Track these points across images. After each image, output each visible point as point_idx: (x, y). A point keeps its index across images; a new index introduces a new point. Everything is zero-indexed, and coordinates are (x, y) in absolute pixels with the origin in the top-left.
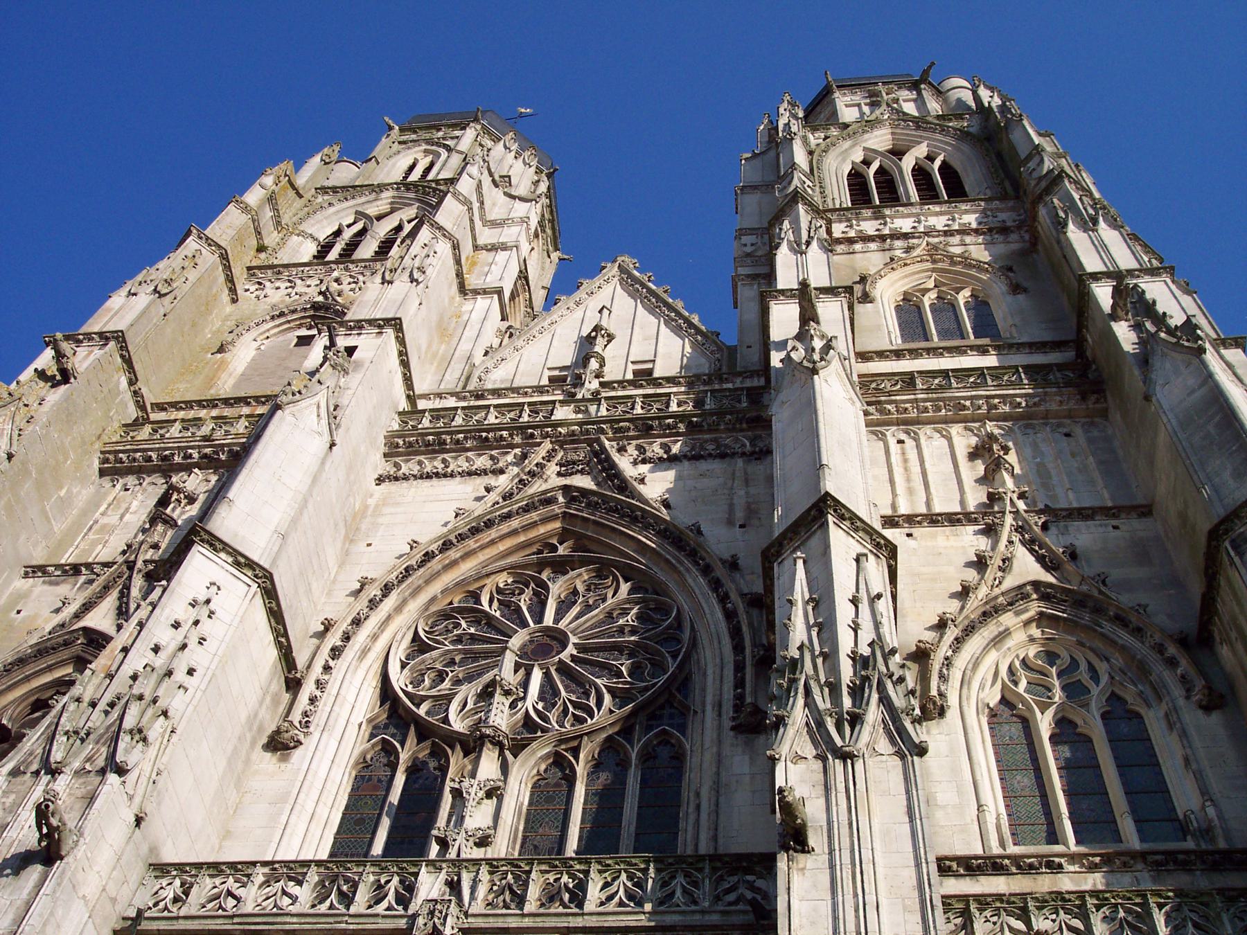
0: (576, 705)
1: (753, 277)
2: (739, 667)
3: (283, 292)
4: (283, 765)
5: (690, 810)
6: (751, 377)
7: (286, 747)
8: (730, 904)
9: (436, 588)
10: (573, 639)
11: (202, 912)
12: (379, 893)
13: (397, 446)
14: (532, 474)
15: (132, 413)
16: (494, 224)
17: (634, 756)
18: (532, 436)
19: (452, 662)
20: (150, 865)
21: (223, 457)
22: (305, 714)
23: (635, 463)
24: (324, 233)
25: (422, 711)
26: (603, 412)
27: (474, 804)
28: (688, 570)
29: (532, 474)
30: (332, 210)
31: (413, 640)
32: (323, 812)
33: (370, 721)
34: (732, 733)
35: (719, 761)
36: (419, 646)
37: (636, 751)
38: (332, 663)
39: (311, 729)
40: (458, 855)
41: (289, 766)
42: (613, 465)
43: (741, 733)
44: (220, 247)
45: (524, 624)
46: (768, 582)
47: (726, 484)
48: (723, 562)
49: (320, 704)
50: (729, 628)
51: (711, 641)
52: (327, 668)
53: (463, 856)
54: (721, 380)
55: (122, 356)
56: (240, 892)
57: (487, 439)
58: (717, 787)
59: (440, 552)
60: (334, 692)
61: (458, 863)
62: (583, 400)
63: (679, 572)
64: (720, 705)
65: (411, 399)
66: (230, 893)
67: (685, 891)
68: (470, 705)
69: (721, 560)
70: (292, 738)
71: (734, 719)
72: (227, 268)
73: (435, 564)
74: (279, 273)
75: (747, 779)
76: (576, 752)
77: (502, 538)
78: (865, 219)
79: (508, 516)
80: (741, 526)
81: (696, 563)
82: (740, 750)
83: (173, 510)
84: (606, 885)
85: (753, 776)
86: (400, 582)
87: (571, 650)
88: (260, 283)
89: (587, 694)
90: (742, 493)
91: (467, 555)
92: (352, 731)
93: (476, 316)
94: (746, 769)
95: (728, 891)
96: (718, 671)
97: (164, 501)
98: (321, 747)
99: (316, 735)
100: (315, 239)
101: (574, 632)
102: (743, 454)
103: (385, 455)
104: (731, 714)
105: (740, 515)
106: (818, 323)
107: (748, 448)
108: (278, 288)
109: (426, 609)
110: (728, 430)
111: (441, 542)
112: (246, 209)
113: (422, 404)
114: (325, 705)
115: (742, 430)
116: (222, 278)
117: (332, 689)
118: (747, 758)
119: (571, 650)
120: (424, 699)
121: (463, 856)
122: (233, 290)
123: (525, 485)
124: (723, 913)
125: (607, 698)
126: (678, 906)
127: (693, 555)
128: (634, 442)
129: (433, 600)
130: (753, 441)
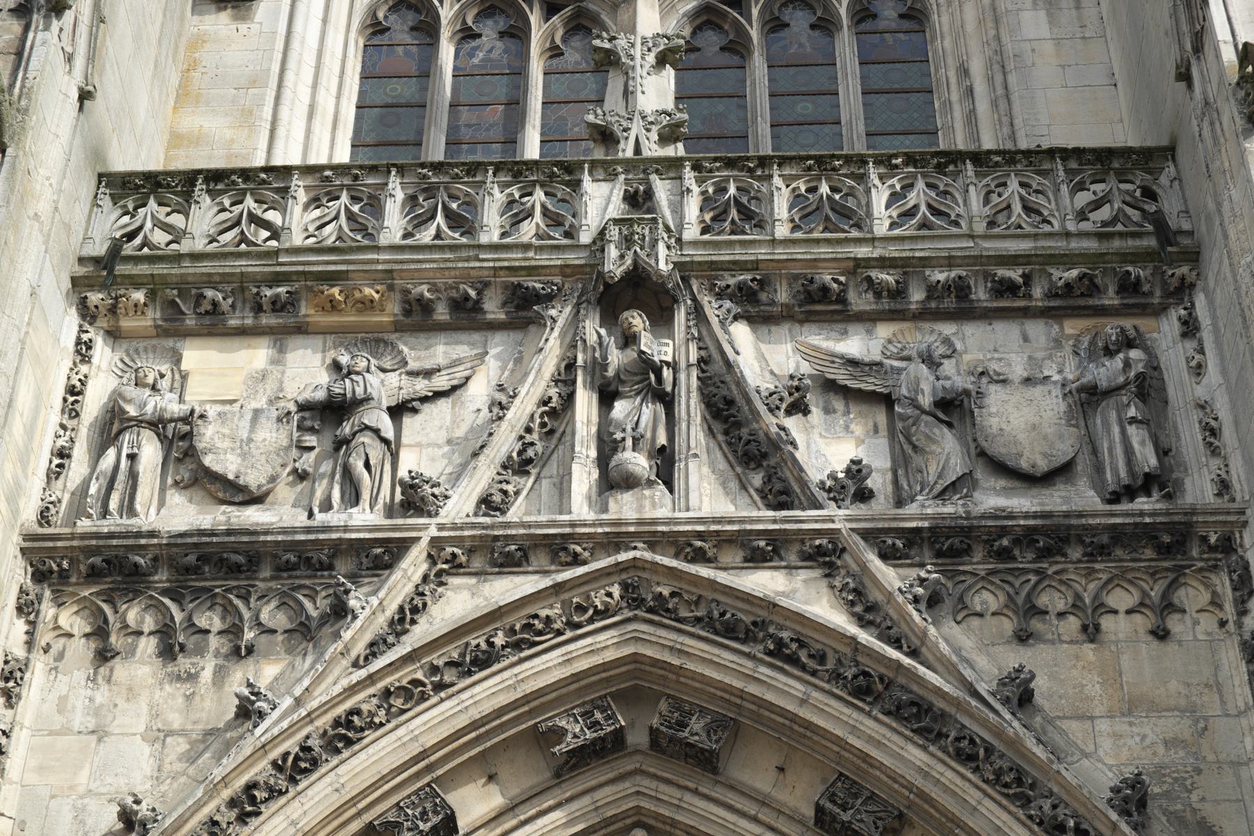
4: (243, 27)
5: (955, 97)
8: (1105, 224)
12: (516, 215)
17: (843, 11)
20: (100, 176)
32: (326, 102)
40: (638, 150)
53: (646, 153)
56: (273, 216)
58: (999, 63)
61: (641, 165)
66: (254, 219)
67: (1028, 209)
75: (1049, 47)
84: (894, 198)
85: (1058, 41)
94: (1044, 31)
95: (1097, 205)
118: (1042, 14)
121: (646, 153)
124: (1101, 236)
126: (1020, 227)
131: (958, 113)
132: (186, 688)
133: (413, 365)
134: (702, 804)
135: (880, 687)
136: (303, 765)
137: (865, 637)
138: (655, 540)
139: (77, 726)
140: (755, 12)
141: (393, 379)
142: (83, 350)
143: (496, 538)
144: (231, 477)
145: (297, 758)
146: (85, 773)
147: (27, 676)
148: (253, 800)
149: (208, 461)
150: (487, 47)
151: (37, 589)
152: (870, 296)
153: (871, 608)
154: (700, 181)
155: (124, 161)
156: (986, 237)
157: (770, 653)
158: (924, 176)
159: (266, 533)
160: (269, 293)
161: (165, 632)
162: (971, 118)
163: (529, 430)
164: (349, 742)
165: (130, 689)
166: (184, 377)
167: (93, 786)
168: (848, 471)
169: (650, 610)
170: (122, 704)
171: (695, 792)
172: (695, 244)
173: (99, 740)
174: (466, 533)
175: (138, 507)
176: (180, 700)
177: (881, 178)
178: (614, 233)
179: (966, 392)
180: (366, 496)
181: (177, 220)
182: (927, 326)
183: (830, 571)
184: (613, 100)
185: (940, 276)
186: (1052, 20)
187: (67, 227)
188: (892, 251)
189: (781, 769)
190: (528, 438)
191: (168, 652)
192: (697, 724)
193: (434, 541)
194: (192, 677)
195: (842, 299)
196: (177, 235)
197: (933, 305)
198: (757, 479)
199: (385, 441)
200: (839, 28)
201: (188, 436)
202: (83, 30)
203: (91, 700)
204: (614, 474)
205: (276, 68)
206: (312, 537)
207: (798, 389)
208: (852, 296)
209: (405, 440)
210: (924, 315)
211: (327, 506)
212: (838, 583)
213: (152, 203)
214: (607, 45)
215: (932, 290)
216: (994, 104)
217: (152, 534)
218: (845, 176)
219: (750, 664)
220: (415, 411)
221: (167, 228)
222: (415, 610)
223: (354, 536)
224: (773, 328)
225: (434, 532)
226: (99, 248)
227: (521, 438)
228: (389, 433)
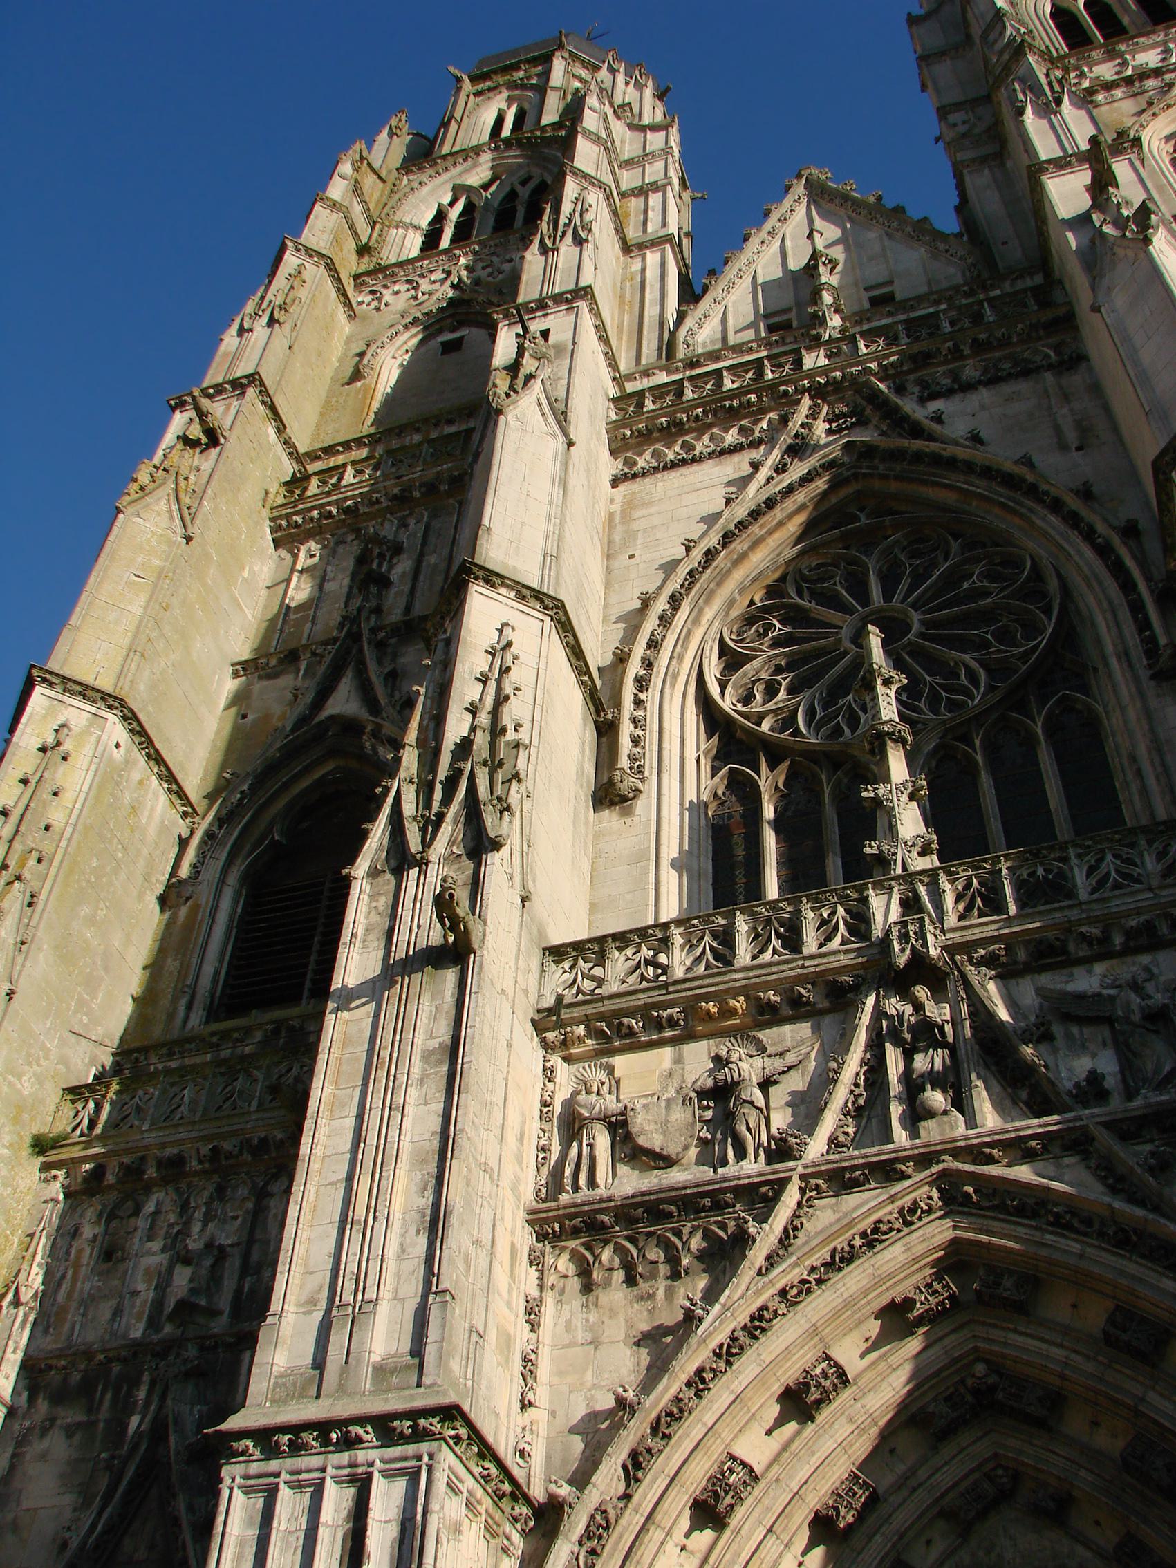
0: (947, 689)
1: (983, 160)
2: (1137, 607)
3: (405, 296)
4: (628, 820)
6: (1021, 277)
7: (625, 799)
10: (915, 617)
11: (624, 988)
12: (827, 929)
15: (288, 468)
16: (628, 164)
17: (1039, 731)
20: (544, 949)
21: (417, 494)
23: (922, 401)
24: (426, 217)
28: (1031, 510)
30: (425, 189)
34: (1153, 683)
35: (1148, 714)
36: (732, 661)
37: (1040, 724)
38: (642, 696)
39: (647, 774)
42: (897, 409)
44: (321, 255)
46: (1164, 498)
50: (1107, 566)
51: (1089, 586)
52: (638, 703)
54: (985, 288)
55: (263, 403)
56: (662, 958)
59: (724, 547)
62: (832, 340)
63: (1021, 516)
64: (1127, 654)
65: (619, 380)
69: (1072, 491)
71: (1150, 667)
72: (337, 279)
74: (393, 274)
76: (967, 739)
78: (1098, 63)
80: (1079, 449)
81: (1041, 501)
83: (380, 565)
84: (1091, 871)
87: (916, 627)
88: (373, 292)
90: (1065, 411)
91: (756, 544)
93: (652, 274)
96: (1109, 616)
97: (362, 560)
100: (416, 228)
101: (914, 606)
102: (1050, 367)
103: (612, 452)
104: (1145, 662)
105: (1072, 437)
106: (1117, 187)
108: (397, 293)
109: (727, 615)
112: (334, 205)
113: (630, 387)
115: (1040, 339)
116: (333, 293)
119: (916, 627)
120: (759, 720)
121: (912, 869)
122: (348, 304)
128: (912, 377)
129: (731, 603)
130: (1057, 349)
131: (1134, 788)
132: (649, 1305)
133: (770, 1050)
134: (1021, 1339)
135: (1134, 1238)
136: (734, 1351)
137: (1117, 1204)
138: (956, 1153)
139: (580, 1340)
140: (977, 742)
141: (758, 1062)
142: (549, 1074)
143: (845, 1169)
144: (658, 1150)
145: (729, 1347)
146: (590, 1372)
147: (543, 1308)
148: (703, 1380)
149: (641, 1141)
151: (540, 1245)
152: (1084, 946)
153: (1121, 1179)
154: (952, 882)
155: (557, 938)
156: (1161, 887)
157: (1051, 1224)
158: (1110, 849)
159: (685, 1188)
160: (665, 1014)
161: (629, 1268)
162: (1144, 791)
163: (857, 1085)
164: (763, 1330)
165: (611, 1310)
166: (618, 1082)
167: (596, 1382)
168: (1087, 1080)
169: (961, 1205)
170: (606, 1320)
171: (1015, 1331)
172: (954, 930)
173: (596, 1348)
174: (823, 1168)
175: (598, 1180)
176: (645, 1313)
177: (1079, 856)
178: (895, 933)
179: (1165, 1006)
180: (751, 1150)
181: (598, 971)
182: (1129, 959)
183: (1085, 1155)
185: (1133, 923)
187: (526, 992)
188: (1097, 910)
189: (1074, 1306)
190: (857, 1092)
191: (630, 1281)
192: (1008, 1282)
193: (802, 1177)
194: (651, 1296)
195: (1064, 951)
196: (600, 982)
197: (1132, 944)
198: (1024, 1094)
199: (760, 1109)
201: (625, 1124)
202: (517, 855)
203: (587, 1320)
204: (919, 1109)
205: (653, 845)
206: (716, 1186)
207: (1043, 1024)
208: (1071, 947)
209: (772, 1105)
210: (1127, 951)
211: (724, 1163)
212: (1093, 1163)
213: (581, 962)
214: (872, 795)
215: (1130, 934)
217: (610, 1199)
218: (1054, 860)
219: (1038, 1234)
220: (776, 1082)
221: (593, 978)
222: (795, 1229)
223: (746, 1181)
224: (1020, 981)
225: (800, 1170)
226: (549, 1002)
227: (852, 1092)
228: (761, 1102)
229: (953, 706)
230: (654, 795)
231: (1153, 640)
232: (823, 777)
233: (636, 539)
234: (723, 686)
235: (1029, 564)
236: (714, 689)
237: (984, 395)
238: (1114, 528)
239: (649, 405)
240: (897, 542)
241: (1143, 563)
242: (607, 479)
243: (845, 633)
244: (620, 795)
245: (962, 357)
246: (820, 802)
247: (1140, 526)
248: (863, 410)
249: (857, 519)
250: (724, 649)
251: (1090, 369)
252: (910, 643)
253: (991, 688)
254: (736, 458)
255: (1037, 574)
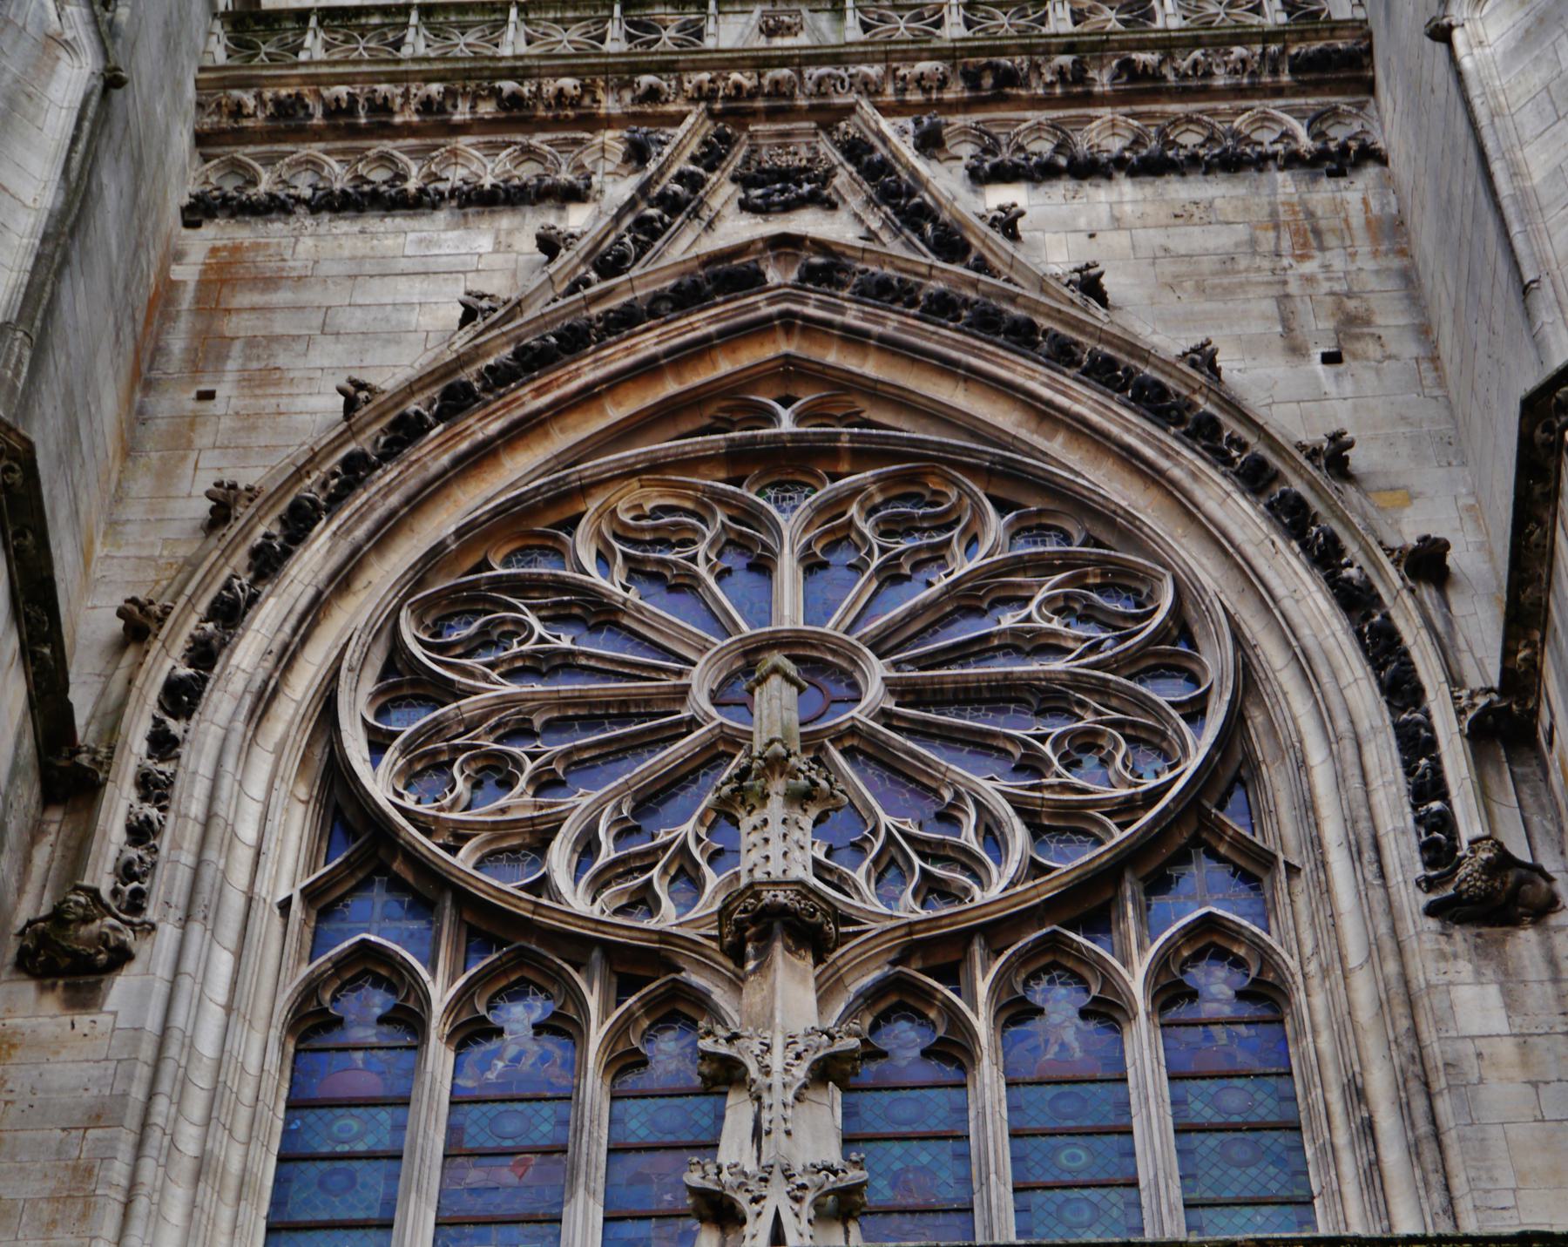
0: (930, 851)
4: (83, 1020)
9: (441, 523)
10: (876, 673)
13: (238, 111)
14: (672, 205)
18: (653, 94)
19: (522, 731)
22: (126, 872)
23: (980, 177)
25: (464, 860)
26: (852, 31)
27: (790, 1098)
29: (672, 205)
31: (388, 669)
33: (311, 894)
34: (1432, 924)
38: (175, 727)
39: (151, 914)
41: (104, 1020)
43: (1461, 921)
45: (724, 626)
47: (1253, 242)
48: (1313, 454)
49: (164, 843)
50: (1359, 635)
52: (162, 744)
57: (516, 99)
60: (196, 809)
68: (608, 852)
70: (103, 939)
71: (1429, 884)
73: (433, 455)
75: (1507, 1049)
76: (952, 974)
77: (616, 382)
79: (626, 320)
80: (1331, 359)
81: (1220, 457)
82: (1465, 968)
85: (1523, 1040)
86: (336, 501)
87: (874, 693)
89: (948, 818)
92: (267, 923)
94: (1498, 1022)
98: (189, 965)
99: (168, 934)
101: (879, 645)
102: (1293, 160)
103: (202, 139)
104: (1419, 870)
105: (1319, 331)
107: (1305, 143)
109: (419, 584)
110: (1237, 92)
111: (435, 391)
114: (176, 845)
115: (1278, 92)
117: (191, 800)
118: (1493, 991)
119: (874, 693)
120: (458, 837)
123: (655, 235)
125: (1019, 837)
127: (1204, 434)
128: (959, 120)
129: (435, 558)
130: (1317, 121)
131: (1348, 1166)
140: (983, 987)
150: (512, 1051)
184: (735, 1148)
186: (1511, 1003)
200: (1130, 1016)
205: (138, 1092)
214: (723, 1049)
216: (1414, 1151)
229: (932, 889)
230: (163, 971)
231: (1445, 821)
232: (593, 1002)
233: (222, 357)
234: (378, 744)
235: (1167, 601)
236: (356, 748)
237: (1125, 193)
238: (1390, 551)
239: (314, 45)
240: (856, 491)
241: (1445, 651)
242: (179, 196)
243: (701, 680)
244: (75, 954)
245: (1089, 99)
246: (576, 1067)
247: (1450, 561)
248: (830, 173)
249: (770, 418)
250: (397, 658)
251: (1388, 183)
252: (853, 731)
253: (1036, 869)
254: (505, 221)
255: (1180, 627)
